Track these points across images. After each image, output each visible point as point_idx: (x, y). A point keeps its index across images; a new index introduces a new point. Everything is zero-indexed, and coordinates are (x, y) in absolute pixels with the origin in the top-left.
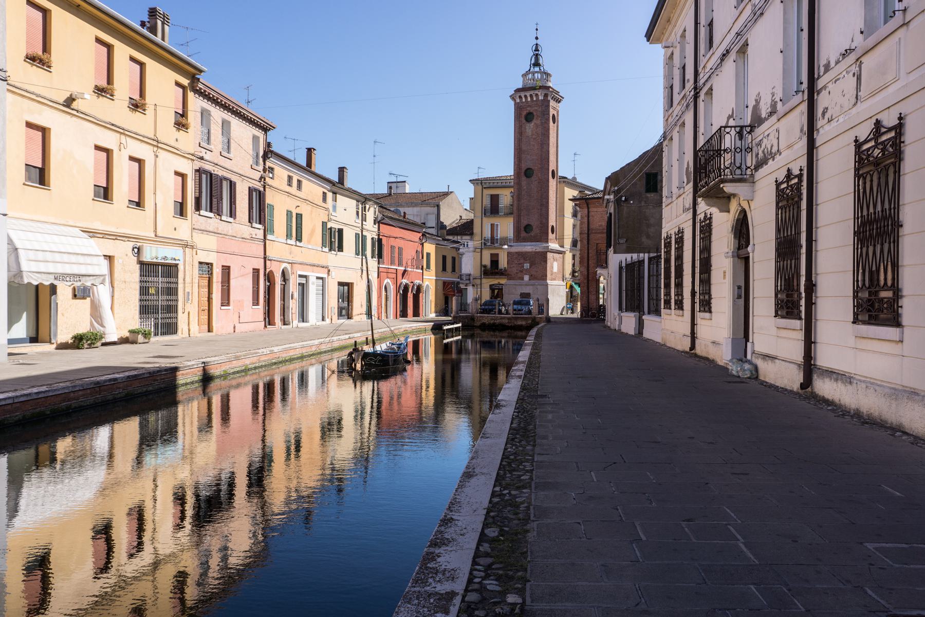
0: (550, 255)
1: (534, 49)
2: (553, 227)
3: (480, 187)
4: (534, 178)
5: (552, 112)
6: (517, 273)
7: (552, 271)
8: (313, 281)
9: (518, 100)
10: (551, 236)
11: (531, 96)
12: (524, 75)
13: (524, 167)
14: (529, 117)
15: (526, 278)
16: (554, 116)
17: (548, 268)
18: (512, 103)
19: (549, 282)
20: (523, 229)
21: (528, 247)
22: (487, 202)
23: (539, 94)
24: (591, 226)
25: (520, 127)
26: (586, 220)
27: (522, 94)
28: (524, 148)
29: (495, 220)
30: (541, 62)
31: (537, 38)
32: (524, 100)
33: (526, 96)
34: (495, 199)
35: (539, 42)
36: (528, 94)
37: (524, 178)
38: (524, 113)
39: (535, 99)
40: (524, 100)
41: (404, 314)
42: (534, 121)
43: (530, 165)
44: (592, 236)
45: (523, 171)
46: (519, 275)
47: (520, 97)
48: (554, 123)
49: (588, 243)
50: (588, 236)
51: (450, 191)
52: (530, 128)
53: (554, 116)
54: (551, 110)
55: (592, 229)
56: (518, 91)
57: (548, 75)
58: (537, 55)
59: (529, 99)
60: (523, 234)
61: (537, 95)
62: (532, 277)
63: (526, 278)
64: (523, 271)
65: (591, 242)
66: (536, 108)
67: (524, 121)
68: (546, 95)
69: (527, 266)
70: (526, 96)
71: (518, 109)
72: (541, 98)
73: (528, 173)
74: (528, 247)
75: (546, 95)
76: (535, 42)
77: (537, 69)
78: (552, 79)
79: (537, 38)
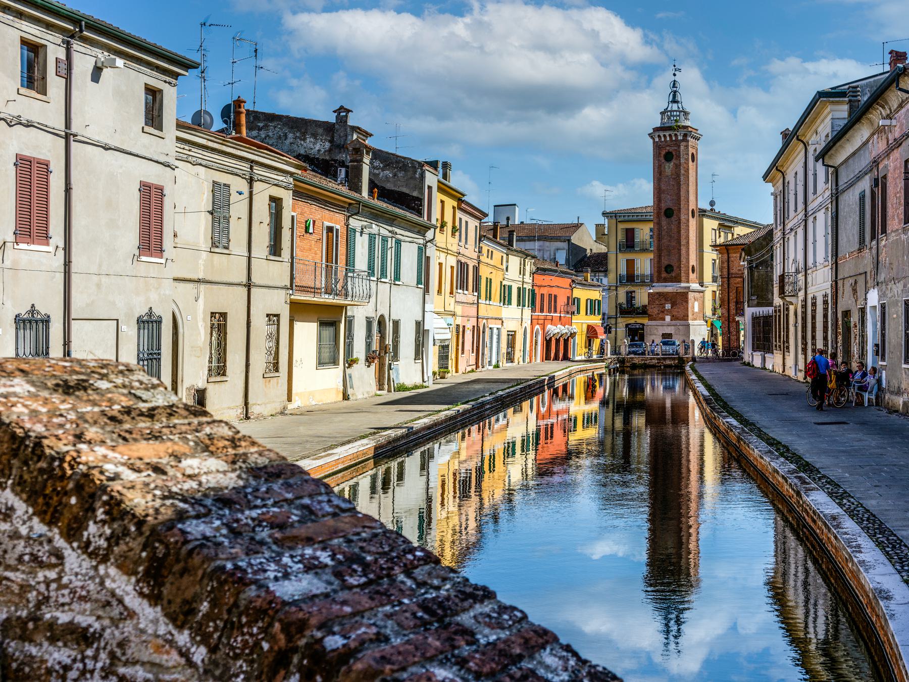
0: (691, 295)
1: (672, 85)
2: (693, 267)
3: (614, 221)
4: (674, 218)
5: (691, 151)
6: (658, 314)
7: (693, 311)
8: (495, 331)
9: (657, 140)
10: (692, 276)
11: (670, 135)
12: (662, 113)
13: (664, 206)
14: (669, 157)
15: (668, 318)
16: (693, 154)
17: (689, 309)
18: (651, 141)
19: (690, 322)
20: (663, 269)
21: (670, 288)
22: (621, 237)
23: (678, 134)
24: (731, 271)
25: (660, 166)
26: (725, 265)
27: (662, 134)
28: (663, 187)
29: (631, 256)
30: (678, 98)
31: (675, 75)
32: (663, 139)
33: (665, 136)
34: (630, 233)
35: (676, 78)
36: (667, 134)
37: (663, 218)
38: (663, 153)
39: (674, 139)
40: (663, 139)
41: (548, 358)
42: (674, 161)
43: (670, 204)
44: (732, 280)
45: (663, 211)
46: (660, 316)
47: (659, 136)
48: (693, 161)
49: (728, 287)
50: (728, 281)
51: (580, 222)
52: (669, 167)
53: (693, 154)
54: (690, 149)
55: (732, 274)
56: (656, 130)
57: (686, 114)
58: (675, 92)
59: (668, 139)
60: (664, 275)
61: (676, 135)
62: (674, 318)
63: (668, 318)
64: (663, 312)
65: (731, 286)
66: (675, 148)
67: (663, 161)
68: (685, 135)
69: (668, 306)
70: (665, 136)
71: (657, 147)
72: (680, 138)
73: (669, 213)
74: (670, 288)
75: (685, 135)
76: (673, 78)
77: (675, 107)
78: (690, 117)
79: (675, 75)
